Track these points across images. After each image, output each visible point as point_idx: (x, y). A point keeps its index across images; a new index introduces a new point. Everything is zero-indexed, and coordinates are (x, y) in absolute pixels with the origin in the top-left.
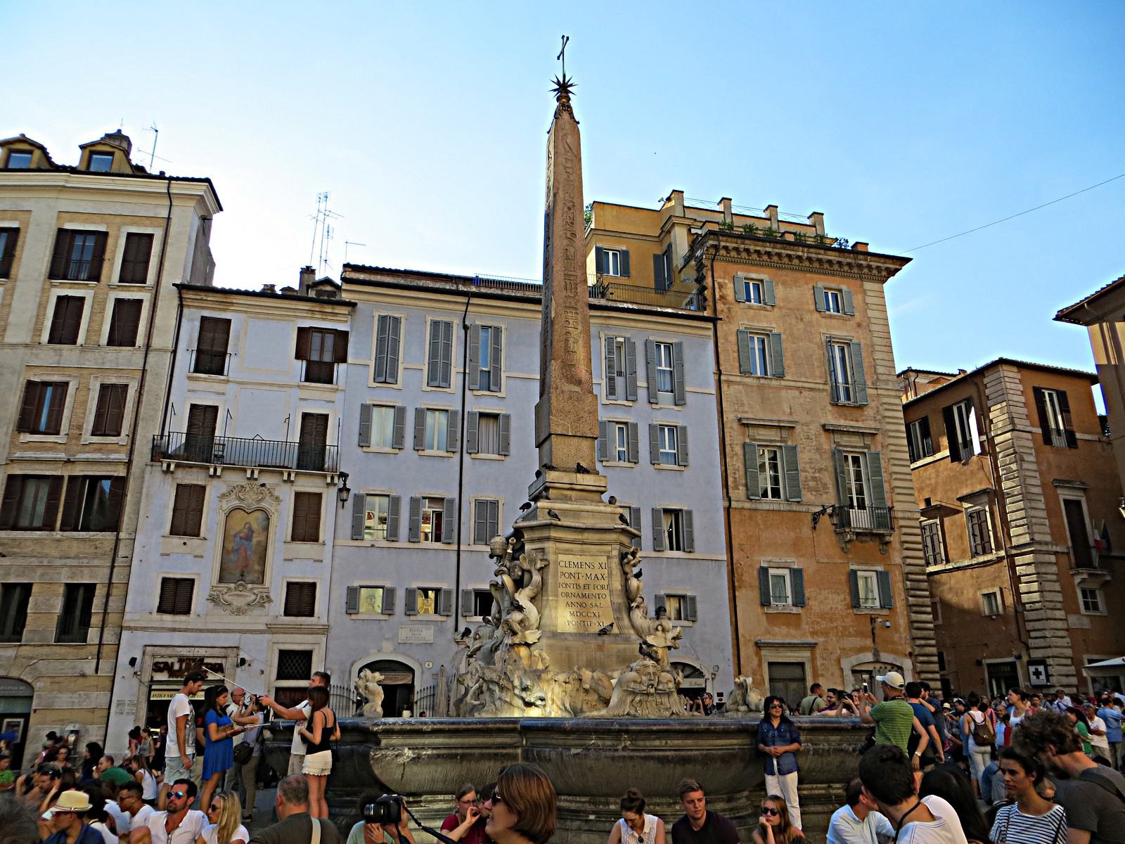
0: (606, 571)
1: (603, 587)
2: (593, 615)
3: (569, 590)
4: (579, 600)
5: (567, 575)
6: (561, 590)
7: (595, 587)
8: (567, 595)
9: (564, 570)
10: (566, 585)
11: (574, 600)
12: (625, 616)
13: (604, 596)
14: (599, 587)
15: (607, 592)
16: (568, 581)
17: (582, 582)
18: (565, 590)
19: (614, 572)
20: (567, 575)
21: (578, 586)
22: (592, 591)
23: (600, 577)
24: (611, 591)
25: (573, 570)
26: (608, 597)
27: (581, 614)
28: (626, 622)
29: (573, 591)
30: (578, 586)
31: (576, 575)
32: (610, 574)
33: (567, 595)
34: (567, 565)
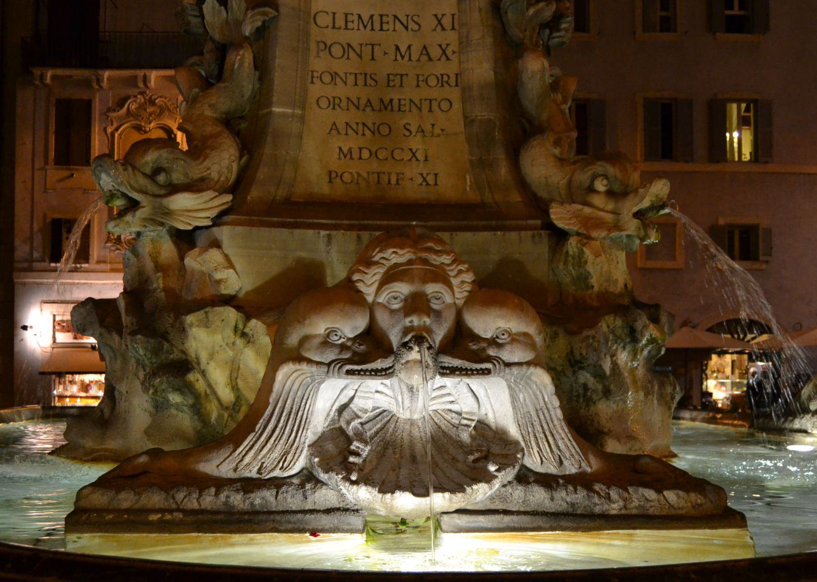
0: (451, 37)
1: (442, 81)
2: (407, 156)
3: (340, 91)
4: (371, 118)
5: (337, 51)
6: (316, 90)
7: (421, 81)
8: (334, 103)
9: (330, 36)
10: (334, 76)
11: (354, 116)
12: (500, 155)
13: (445, 105)
14: (433, 82)
15: (454, 94)
16: (339, 66)
17: (385, 66)
18: (330, 91)
19: (476, 36)
20: (337, 51)
21: (368, 78)
22: (409, 93)
23: (435, 52)
24: (466, 92)
25: (356, 37)
26: (457, 106)
27: (374, 154)
28: (503, 171)
29: (353, 93)
30: (368, 78)
31: (367, 51)
32: (464, 44)
33: (334, 103)
34: (340, 22)
